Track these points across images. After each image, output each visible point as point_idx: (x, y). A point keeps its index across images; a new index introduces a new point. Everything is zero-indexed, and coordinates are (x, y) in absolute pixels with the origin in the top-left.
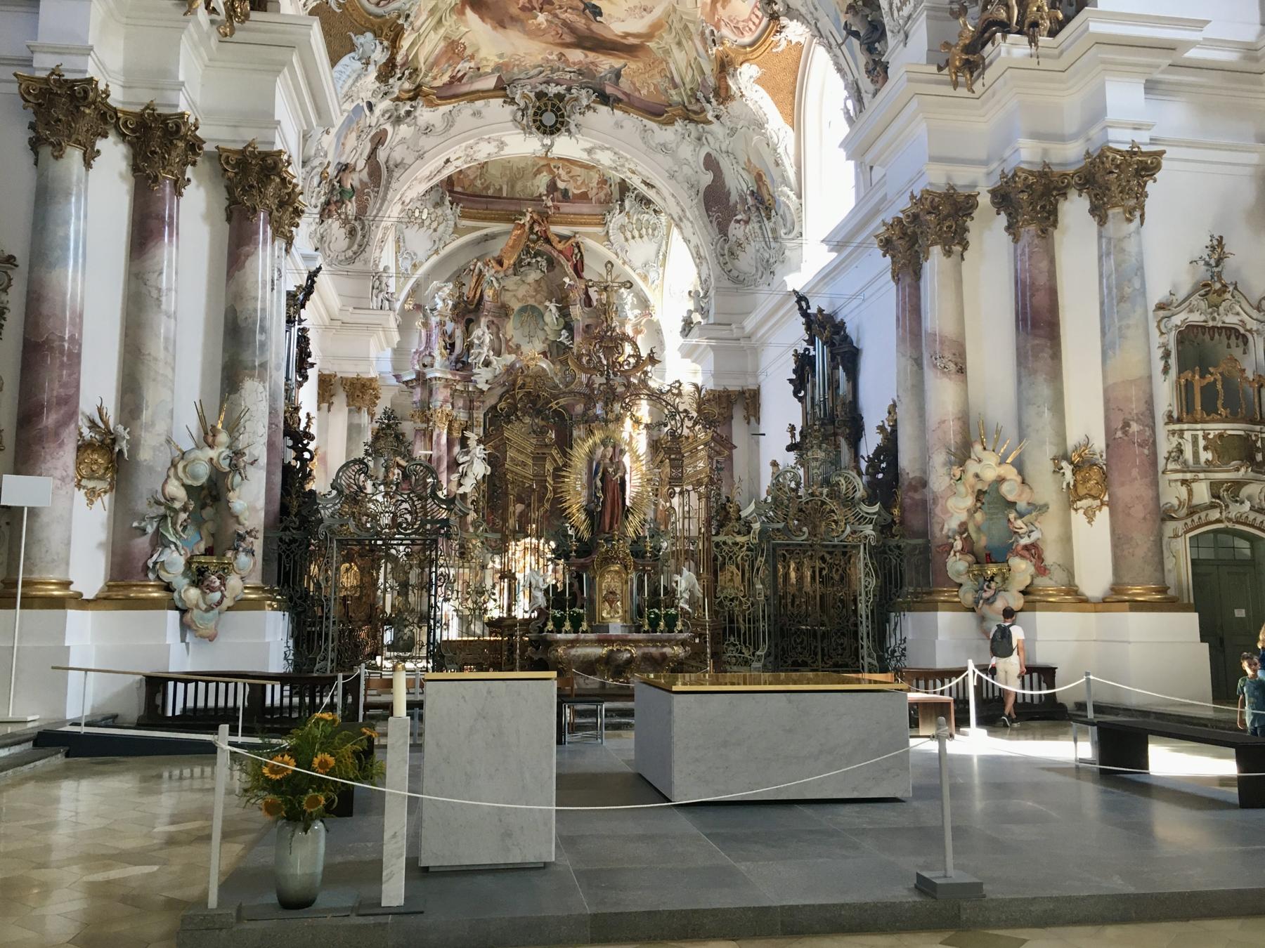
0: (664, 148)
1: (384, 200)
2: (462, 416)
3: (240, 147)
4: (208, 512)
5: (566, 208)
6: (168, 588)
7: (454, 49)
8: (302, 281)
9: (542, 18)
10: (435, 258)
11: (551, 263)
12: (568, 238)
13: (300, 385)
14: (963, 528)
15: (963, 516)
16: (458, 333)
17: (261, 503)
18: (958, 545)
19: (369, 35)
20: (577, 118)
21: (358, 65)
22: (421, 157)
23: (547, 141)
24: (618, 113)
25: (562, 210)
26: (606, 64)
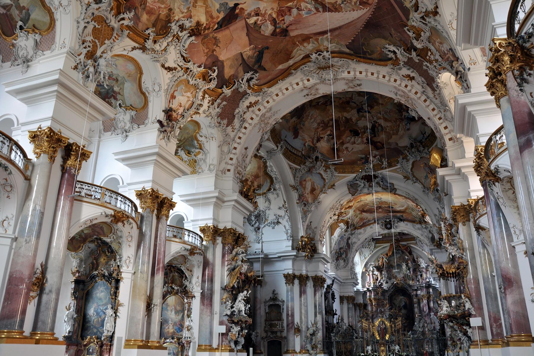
0: (419, 229)
1: (352, 251)
2: (382, 298)
3: (314, 275)
4: (314, 338)
5: (404, 237)
6: (308, 350)
7: (362, 219)
8: (331, 283)
9: (380, 210)
10: (370, 255)
11: (402, 252)
12: (406, 245)
13: (333, 303)
14: (450, 335)
15: (450, 333)
16: (379, 275)
17: (321, 336)
18: (449, 339)
19: (342, 223)
20: (396, 224)
21: (340, 230)
22: (359, 240)
23: (389, 231)
24: (405, 222)
25: (403, 238)
26: (398, 215)
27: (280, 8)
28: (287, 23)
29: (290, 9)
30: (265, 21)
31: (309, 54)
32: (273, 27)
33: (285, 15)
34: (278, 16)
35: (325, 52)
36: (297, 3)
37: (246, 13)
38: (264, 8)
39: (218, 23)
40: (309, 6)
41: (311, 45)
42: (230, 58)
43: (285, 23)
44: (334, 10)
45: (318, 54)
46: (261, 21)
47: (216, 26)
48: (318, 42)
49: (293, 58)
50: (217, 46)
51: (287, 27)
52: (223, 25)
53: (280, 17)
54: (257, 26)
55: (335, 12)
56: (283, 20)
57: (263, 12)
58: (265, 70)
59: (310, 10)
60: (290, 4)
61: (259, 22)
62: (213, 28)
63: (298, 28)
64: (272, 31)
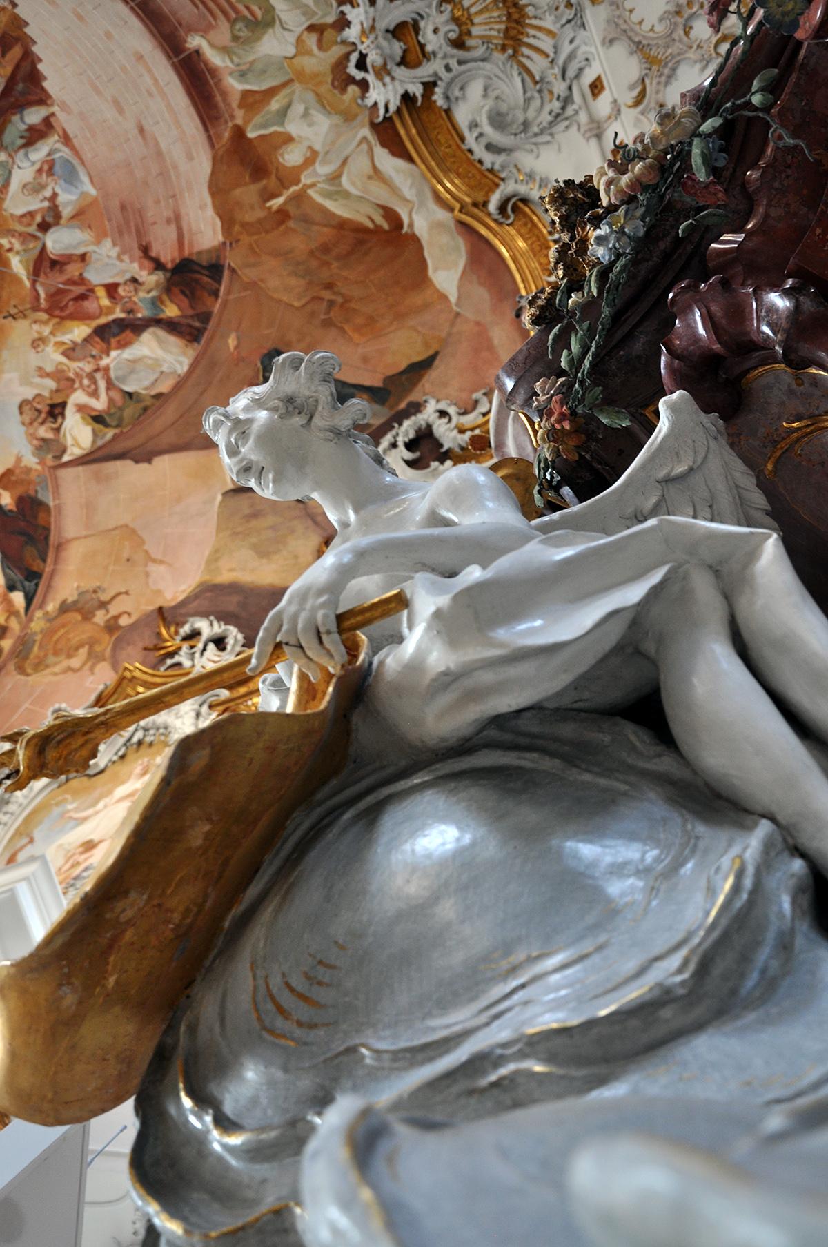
27: (36, 308)
28: (135, 268)
29: (44, 264)
30: (98, 376)
31: (374, 126)
32: (147, 336)
33: (81, 280)
34: (83, 317)
35: (352, 33)
36: (10, 233)
37: (30, 460)
38: (25, 381)
39: (11, 587)
40: (23, 173)
41: (293, 127)
42: (217, 551)
43: (134, 280)
44: (16, 52)
45: (359, 75)
46: (95, 394)
47: (18, 598)
48: (271, 92)
49: (391, 216)
50: (103, 605)
51: (158, 265)
52: (36, 565)
53: (89, 305)
54: (121, 409)
55: (27, 42)
56: (111, 289)
57: (51, 384)
58: (420, 368)
59: (49, 167)
60: (18, 265)
61: (100, 404)
62: (11, 612)
63: (168, 213)
64: (173, 340)
